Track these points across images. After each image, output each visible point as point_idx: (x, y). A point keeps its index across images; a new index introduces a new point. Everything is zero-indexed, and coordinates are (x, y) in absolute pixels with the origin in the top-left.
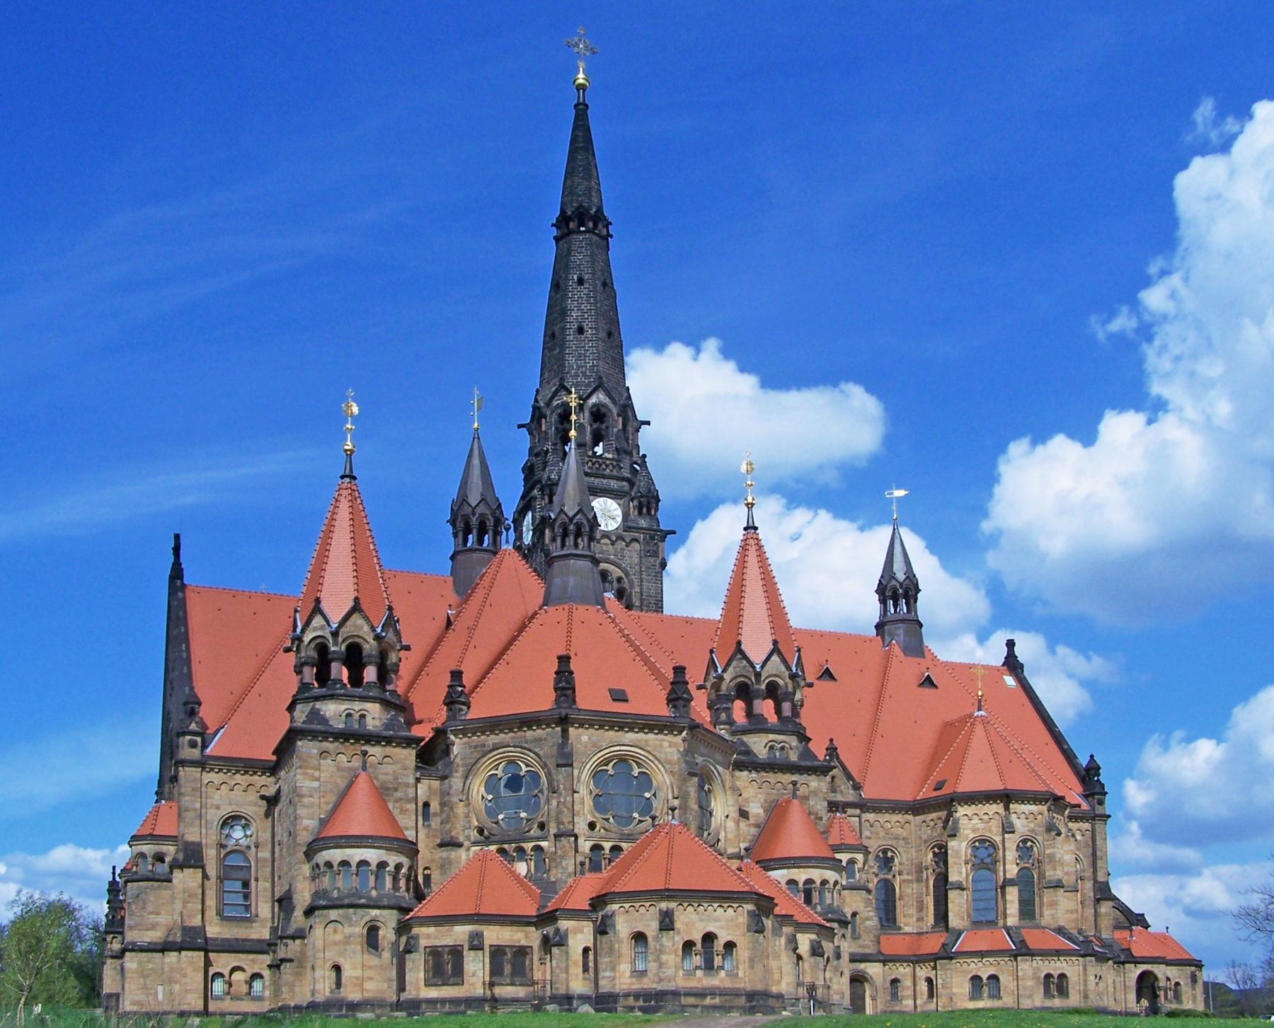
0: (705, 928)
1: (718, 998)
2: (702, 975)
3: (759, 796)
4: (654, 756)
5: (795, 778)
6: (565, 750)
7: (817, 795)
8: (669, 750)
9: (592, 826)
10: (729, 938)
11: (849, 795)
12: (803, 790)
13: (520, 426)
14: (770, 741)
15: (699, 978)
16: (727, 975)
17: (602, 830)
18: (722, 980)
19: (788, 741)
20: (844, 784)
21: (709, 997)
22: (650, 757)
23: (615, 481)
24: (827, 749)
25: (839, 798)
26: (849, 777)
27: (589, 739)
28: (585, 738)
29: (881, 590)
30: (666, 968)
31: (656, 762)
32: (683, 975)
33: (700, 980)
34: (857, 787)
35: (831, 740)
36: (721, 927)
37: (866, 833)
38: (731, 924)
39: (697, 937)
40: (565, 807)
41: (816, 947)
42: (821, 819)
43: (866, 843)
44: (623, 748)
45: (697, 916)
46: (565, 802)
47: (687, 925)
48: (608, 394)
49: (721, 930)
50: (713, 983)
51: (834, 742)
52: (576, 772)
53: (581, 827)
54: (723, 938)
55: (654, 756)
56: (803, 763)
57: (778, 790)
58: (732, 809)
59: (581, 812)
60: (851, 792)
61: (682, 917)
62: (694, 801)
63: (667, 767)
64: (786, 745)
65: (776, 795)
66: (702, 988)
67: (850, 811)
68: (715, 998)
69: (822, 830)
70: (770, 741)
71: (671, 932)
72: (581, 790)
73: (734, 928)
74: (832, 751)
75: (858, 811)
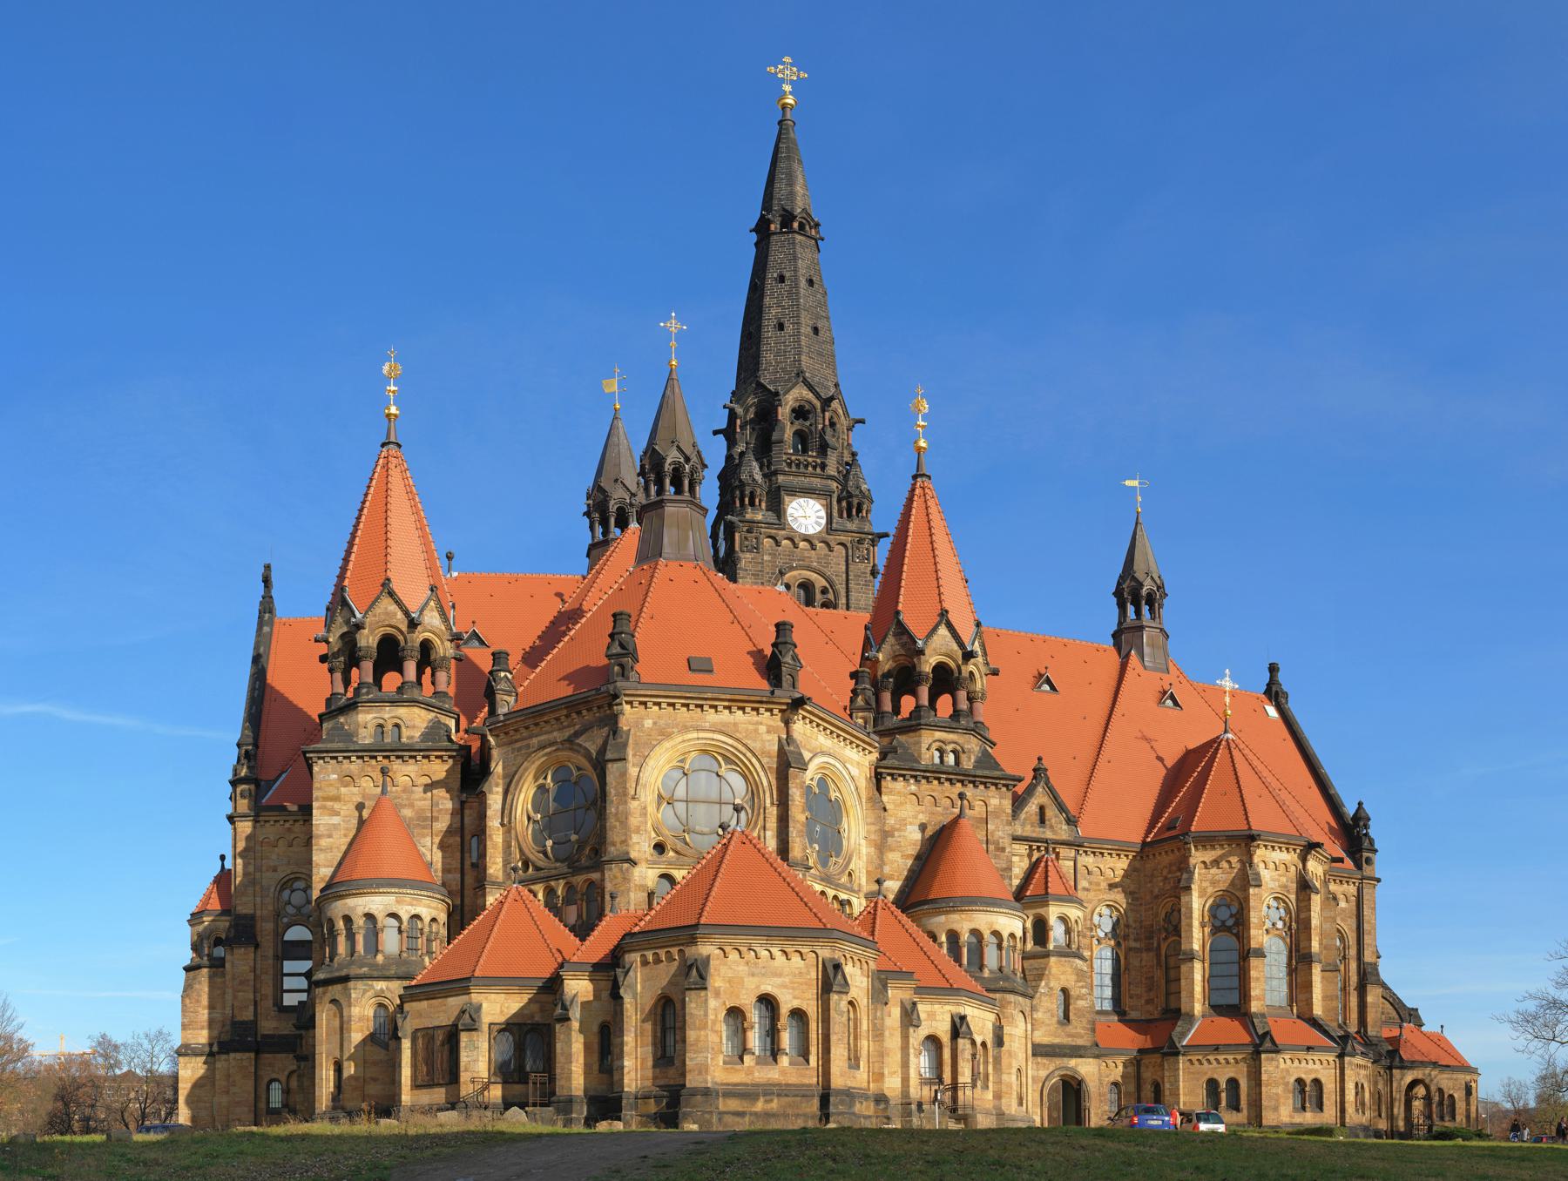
0: (758, 987)
1: (776, 1101)
2: (753, 1064)
3: (921, 816)
4: (745, 745)
5: (970, 791)
6: (619, 740)
7: (998, 817)
8: (769, 737)
9: (660, 848)
10: (796, 1004)
11: (1063, 831)
12: (979, 809)
13: (716, 433)
14: (935, 741)
15: (749, 1067)
16: (790, 1064)
17: (671, 854)
18: (783, 1072)
19: (960, 742)
20: (1056, 816)
21: (762, 1099)
22: (740, 747)
23: (819, 480)
24: (1035, 770)
25: (1049, 835)
26: (1062, 808)
27: (655, 723)
28: (648, 723)
29: (1118, 594)
30: (696, 1052)
31: (749, 755)
32: (725, 1063)
33: (750, 1072)
34: (1071, 821)
35: (1040, 759)
36: (784, 986)
37: (1083, 883)
38: (797, 980)
39: (747, 1001)
40: (617, 820)
41: (957, 1021)
42: (1003, 850)
43: (1081, 894)
44: (702, 735)
45: (746, 968)
46: (616, 814)
47: (729, 982)
48: (811, 388)
49: (784, 990)
50: (769, 1076)
51: (1043, 762)
52: (633, 771)
53: (641, 846)
54: (787, 1003)
55: (745, 745)
56: (979, 773)
57: (947, 809)
58: (873, 828)
59: (642, 828)
60: (1065, 827)
61: (723, 970)
62: (800, 809)
63: (764, 761)
64: (958, 748)
65: (942, 815)
66: (753, 1085)
67: (1065, 852)
68: (772, 1101)
69: (1004, 866)
70: (935, 741)
71: (703, 993)
72: (643, 795)
73: (805, 987)
74: (1039, 772)
75: (1073, 853)
